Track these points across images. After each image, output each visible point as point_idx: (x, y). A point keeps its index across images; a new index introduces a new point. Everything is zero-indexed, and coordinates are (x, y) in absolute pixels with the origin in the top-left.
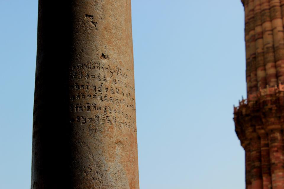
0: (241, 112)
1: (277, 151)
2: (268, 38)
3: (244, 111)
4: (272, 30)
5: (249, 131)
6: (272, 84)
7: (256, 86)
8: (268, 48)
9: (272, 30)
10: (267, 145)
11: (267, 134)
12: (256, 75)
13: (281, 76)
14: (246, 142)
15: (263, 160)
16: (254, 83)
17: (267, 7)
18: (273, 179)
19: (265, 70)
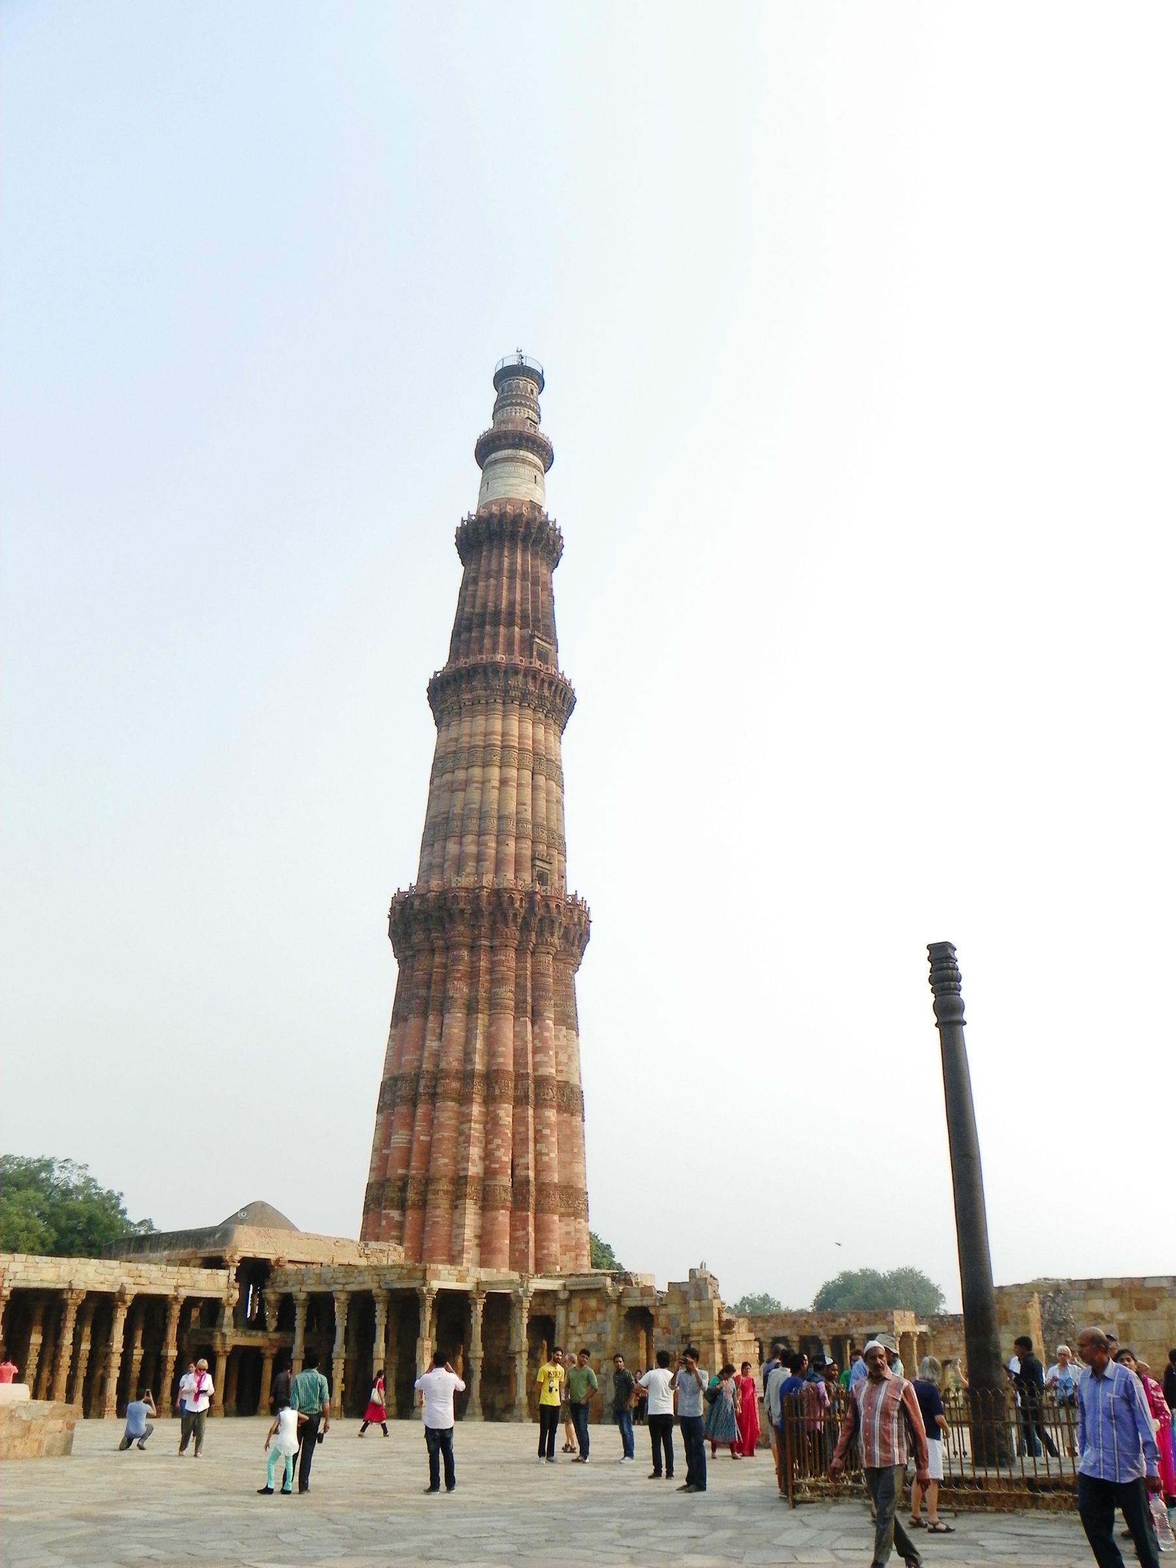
0: (412, 904)
1: (460, 979)
2: (475, 794)
3: (417, 903)
4: (483, 783)
5: (418, 937)
6: (468, 870)
7: (441, 866)
8: (470, 809)
9: (483, 783)
10: (445, 966)
11: (447, 949)
12: (444, 847)
13: (485, 860)
14: (409, 953)
15: (433, 987)
16: (437, 860)
17: (481, 743)
18: (445, 1022)
19: (461, 844)
